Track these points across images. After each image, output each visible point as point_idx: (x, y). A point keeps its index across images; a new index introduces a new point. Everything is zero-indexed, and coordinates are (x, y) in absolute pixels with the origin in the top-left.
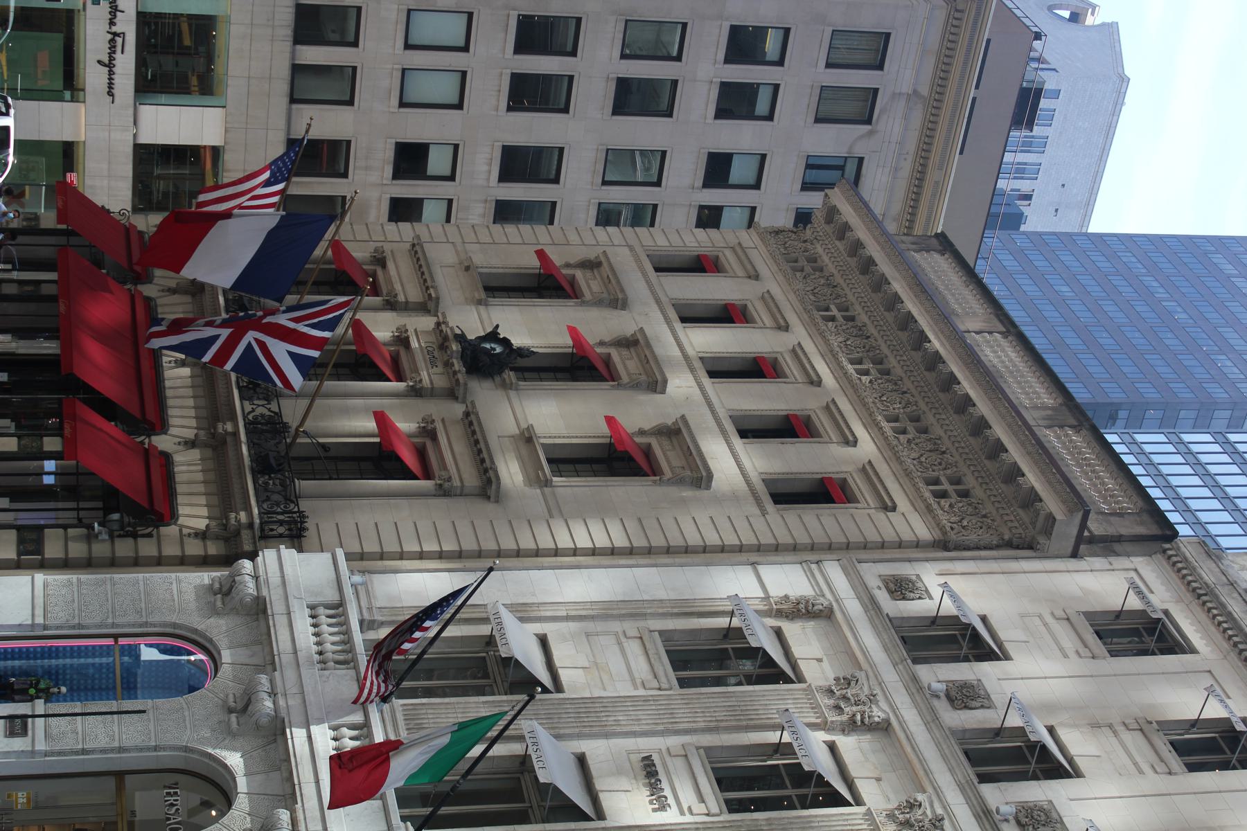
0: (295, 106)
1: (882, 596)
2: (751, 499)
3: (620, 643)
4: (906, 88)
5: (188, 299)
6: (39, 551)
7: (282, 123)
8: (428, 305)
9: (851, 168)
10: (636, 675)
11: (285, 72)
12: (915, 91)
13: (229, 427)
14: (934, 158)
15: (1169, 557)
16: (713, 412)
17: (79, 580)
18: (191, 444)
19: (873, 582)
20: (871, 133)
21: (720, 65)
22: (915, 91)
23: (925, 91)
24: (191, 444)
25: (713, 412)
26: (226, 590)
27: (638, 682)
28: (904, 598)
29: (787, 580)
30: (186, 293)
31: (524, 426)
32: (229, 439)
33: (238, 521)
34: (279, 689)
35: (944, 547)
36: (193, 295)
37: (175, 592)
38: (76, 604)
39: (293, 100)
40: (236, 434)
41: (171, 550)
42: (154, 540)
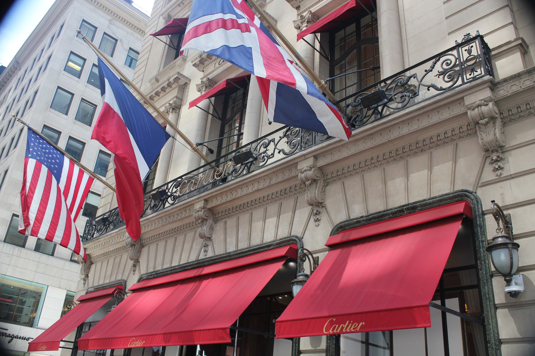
0: (55, 255)
4: (107, 23)
5: (145, 250)
7: (62, 262)
9: (133, 55)
11: (38, 254)
12: (109, 20)
14: (136, 23)
18: (318, 207)
20: (121, 41)
21: (80, 80)
22: (109, 20)
23: (110, 18)
24: (318, 207)
30: (140, 252)
32: (321, 163)
33: (486, 103)
36: (142, 246)
39: (52, 255)
42: (515, 214)
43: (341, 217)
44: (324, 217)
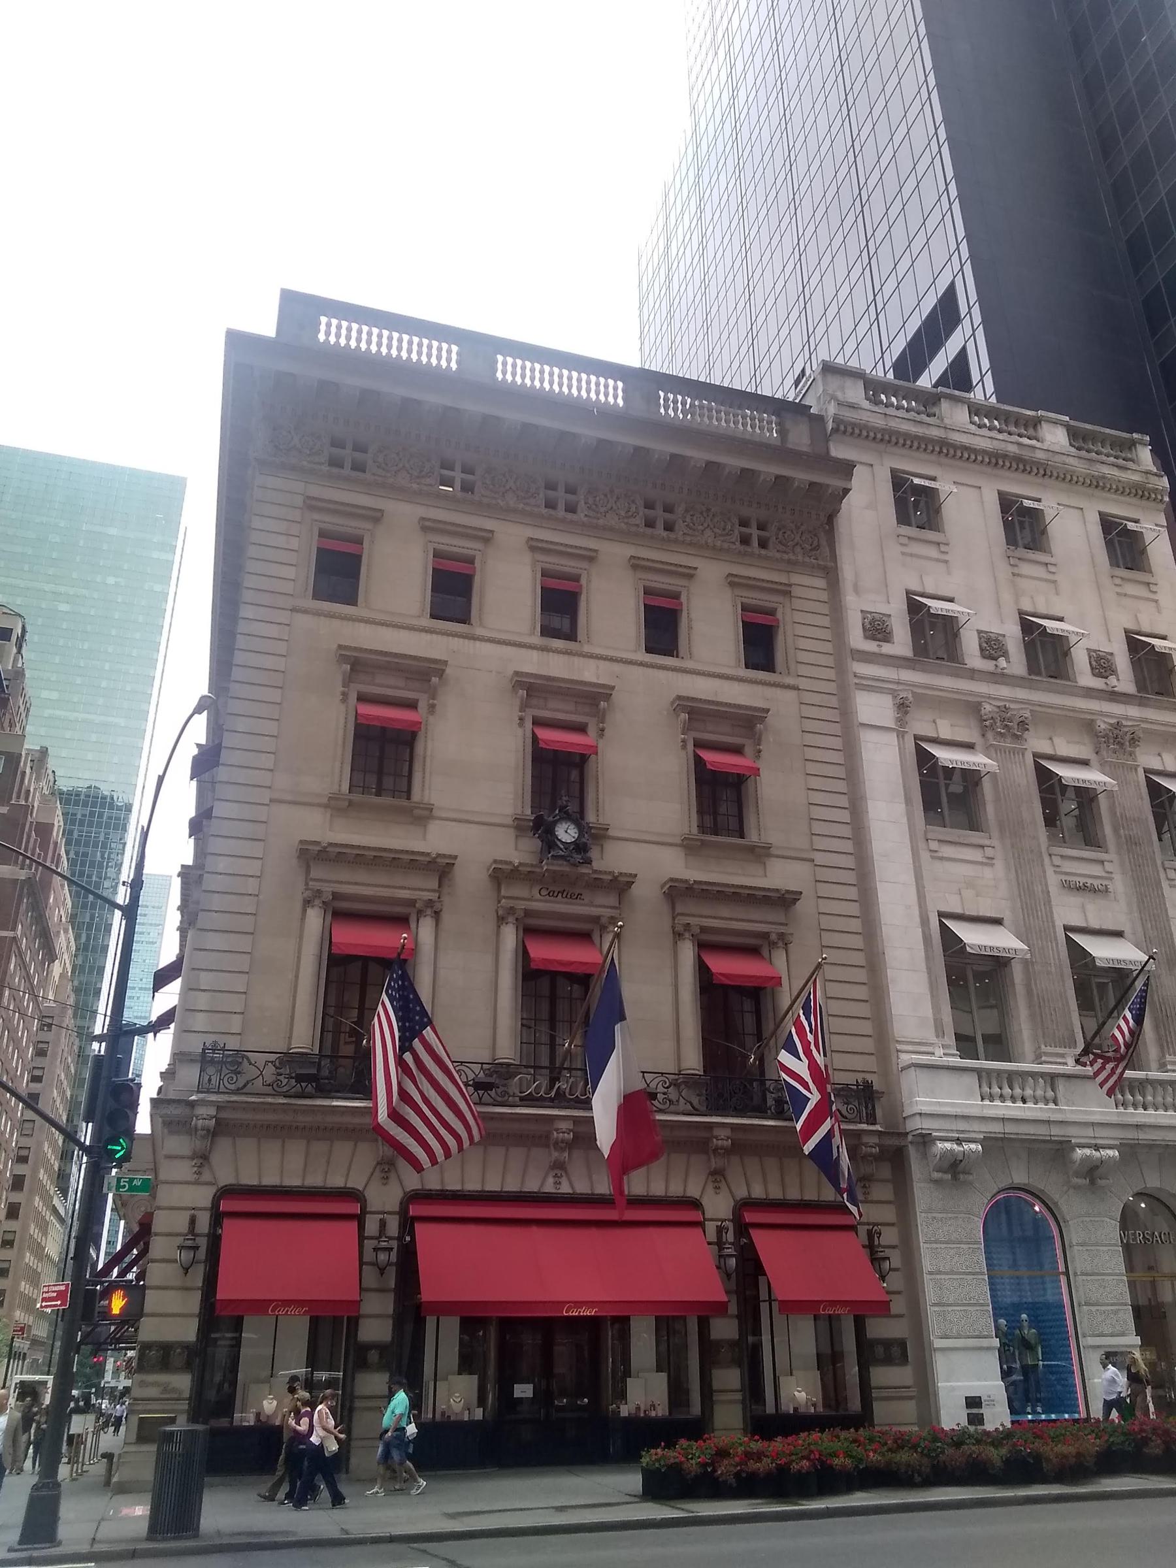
1: (887, 649)
2: (778, 691)
3: (941, 859)
6: (902, 1344)
8: (441, 869)
10: (980, 860)
13: (723, 1133)
15: (845, 432)
16: (641, 664)
17: (935, 1305)
19: (871, 646)
25: (641, 664)
26: (955, 1167)
27: (985, 860)
28: (890, 633)
29: (873, 708)
31: (679, 842)
34: (1093, 1142)
35: (831, 573)
37: (944, 1215)
38: (970, 1308)
40: (733, 1127)
41: (887, 1214)
43: (742, 1193)
44: (723, 1185)
